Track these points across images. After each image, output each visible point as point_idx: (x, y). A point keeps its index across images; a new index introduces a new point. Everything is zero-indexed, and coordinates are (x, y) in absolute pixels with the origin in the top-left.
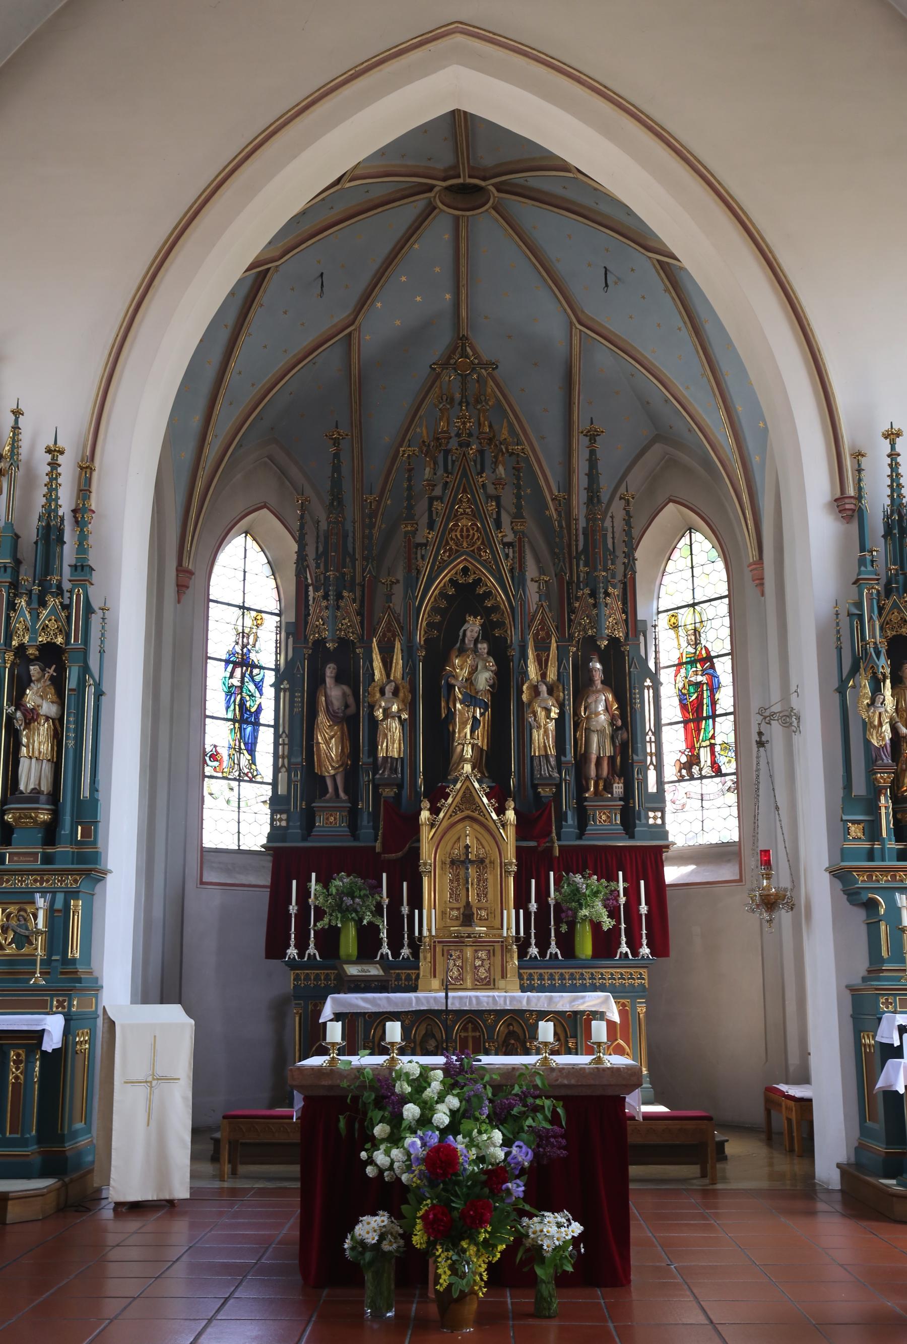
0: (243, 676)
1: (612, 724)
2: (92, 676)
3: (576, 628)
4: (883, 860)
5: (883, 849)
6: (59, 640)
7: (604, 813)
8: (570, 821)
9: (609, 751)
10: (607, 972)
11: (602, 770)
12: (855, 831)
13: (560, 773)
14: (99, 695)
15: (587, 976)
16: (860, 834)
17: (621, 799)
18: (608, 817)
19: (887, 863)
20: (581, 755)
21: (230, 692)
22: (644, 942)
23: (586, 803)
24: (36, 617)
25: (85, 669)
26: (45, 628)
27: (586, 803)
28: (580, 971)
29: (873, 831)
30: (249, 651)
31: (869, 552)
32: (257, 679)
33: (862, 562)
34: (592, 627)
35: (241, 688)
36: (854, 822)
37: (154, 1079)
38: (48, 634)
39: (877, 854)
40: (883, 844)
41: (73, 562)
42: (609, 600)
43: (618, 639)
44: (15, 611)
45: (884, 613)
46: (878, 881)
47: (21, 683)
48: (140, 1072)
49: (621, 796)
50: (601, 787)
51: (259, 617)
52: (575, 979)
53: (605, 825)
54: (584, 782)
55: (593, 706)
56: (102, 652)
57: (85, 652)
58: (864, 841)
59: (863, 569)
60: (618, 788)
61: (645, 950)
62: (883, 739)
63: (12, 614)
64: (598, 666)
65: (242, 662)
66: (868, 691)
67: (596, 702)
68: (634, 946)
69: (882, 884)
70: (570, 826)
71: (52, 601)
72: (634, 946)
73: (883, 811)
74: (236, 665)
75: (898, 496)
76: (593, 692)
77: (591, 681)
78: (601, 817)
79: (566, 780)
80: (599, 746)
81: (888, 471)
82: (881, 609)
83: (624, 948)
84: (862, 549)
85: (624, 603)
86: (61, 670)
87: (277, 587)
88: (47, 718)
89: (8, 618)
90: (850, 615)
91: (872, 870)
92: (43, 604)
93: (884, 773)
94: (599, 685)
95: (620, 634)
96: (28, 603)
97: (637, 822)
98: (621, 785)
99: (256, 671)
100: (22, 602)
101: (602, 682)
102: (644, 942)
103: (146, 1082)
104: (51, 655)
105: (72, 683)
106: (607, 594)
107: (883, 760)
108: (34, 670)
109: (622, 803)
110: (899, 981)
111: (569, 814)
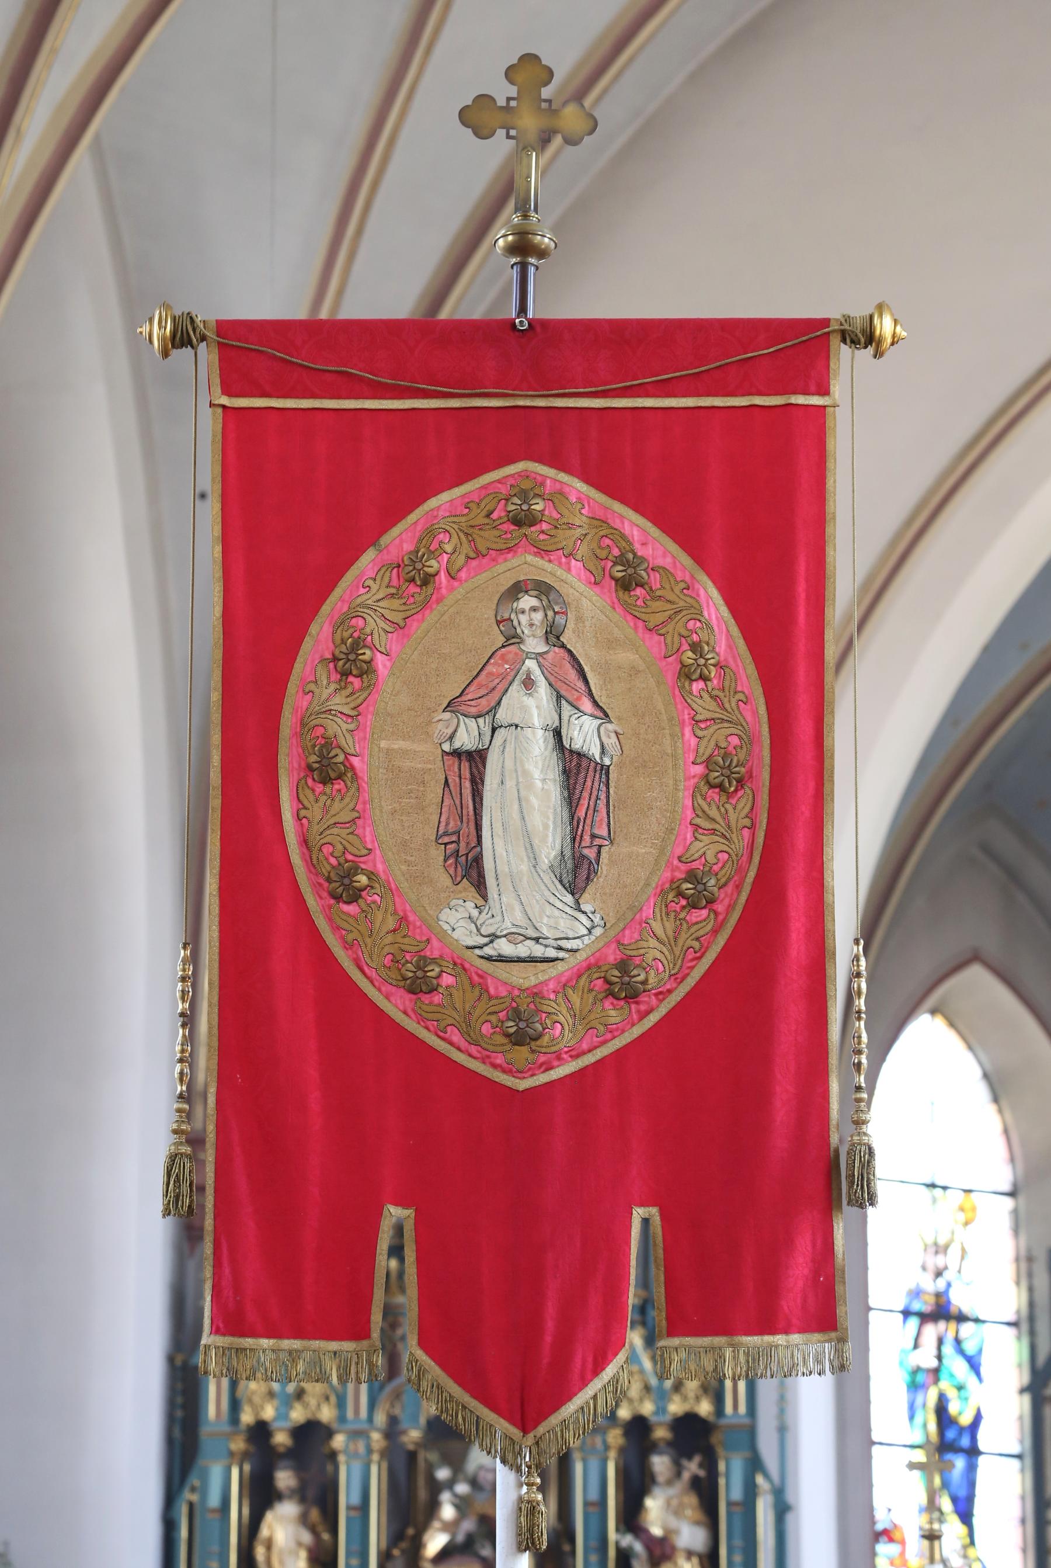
0: (940, 1342)
2: (767, 1476)
6: (705, 1408)
14: (782, 1510)
25: (755, 1464)
30: (949, 1285)
32: (970, 1348)
35: (936, 1372)
38: (685, 1399)
47: (635, 1488)
51: (967, 1206)
56: (782, 1430)
57: (751, 1432)
74: (925, 1318)
86: (710, 1464)
87: (1006, 1131)
88: (690, 1554)
99: (967, 1329)
104: (693, 1436)
105: (731, 1487)
108: (660, 1463)
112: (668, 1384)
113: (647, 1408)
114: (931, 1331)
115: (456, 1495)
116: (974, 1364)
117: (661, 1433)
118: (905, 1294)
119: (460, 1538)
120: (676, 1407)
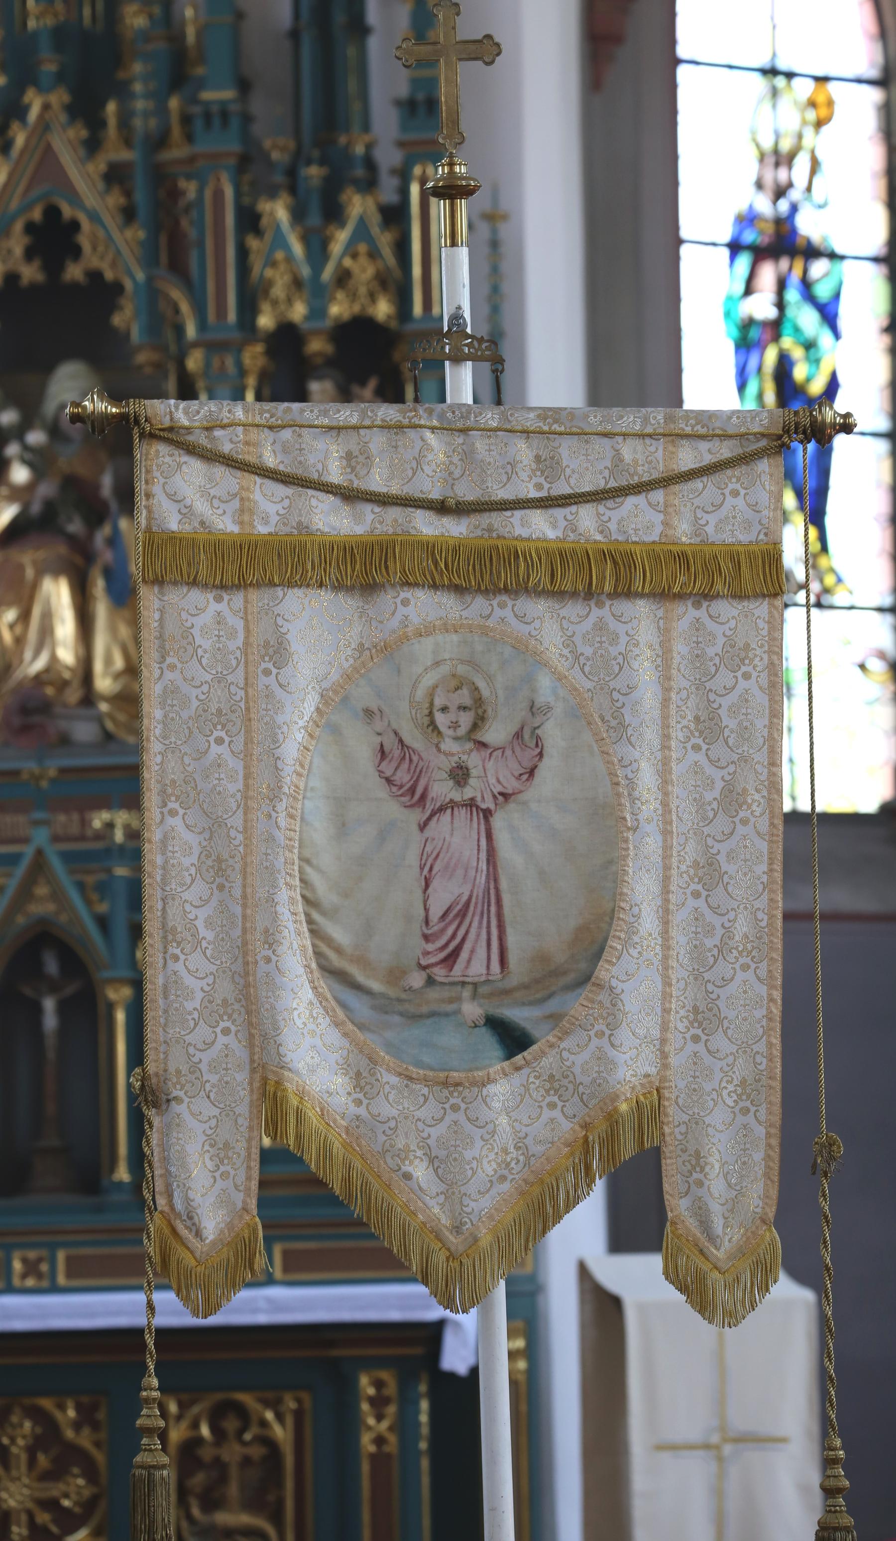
0: (782, 285)
6: (383, 309)
21: (750, 337)
24: (318, 249)
26: (343, 278)
30: (794, 208)
32: (823, 292)
35: (775, 328)
37: (725, 1440)
38: (353, 296)
41: (403, 90)
44: (258, 232)
48: (689, 1421)
51: (821, 99)
63: (253, 243)
65: (777, 244)
71: (358, 205)
74: (760, 254)
89: (243, 253)
92: (334, 213)
96: (298, 215)
99: (818, 268)
100: (278, 211)
103: (707, 1447)
112: (327, 274)
113: (298, 311)
114: (768, 274)
115: (26, 447)
116: (828, 315)
117: (316, 346)
118: (732, 219)
119: (36, 508)
120: (338, 309)
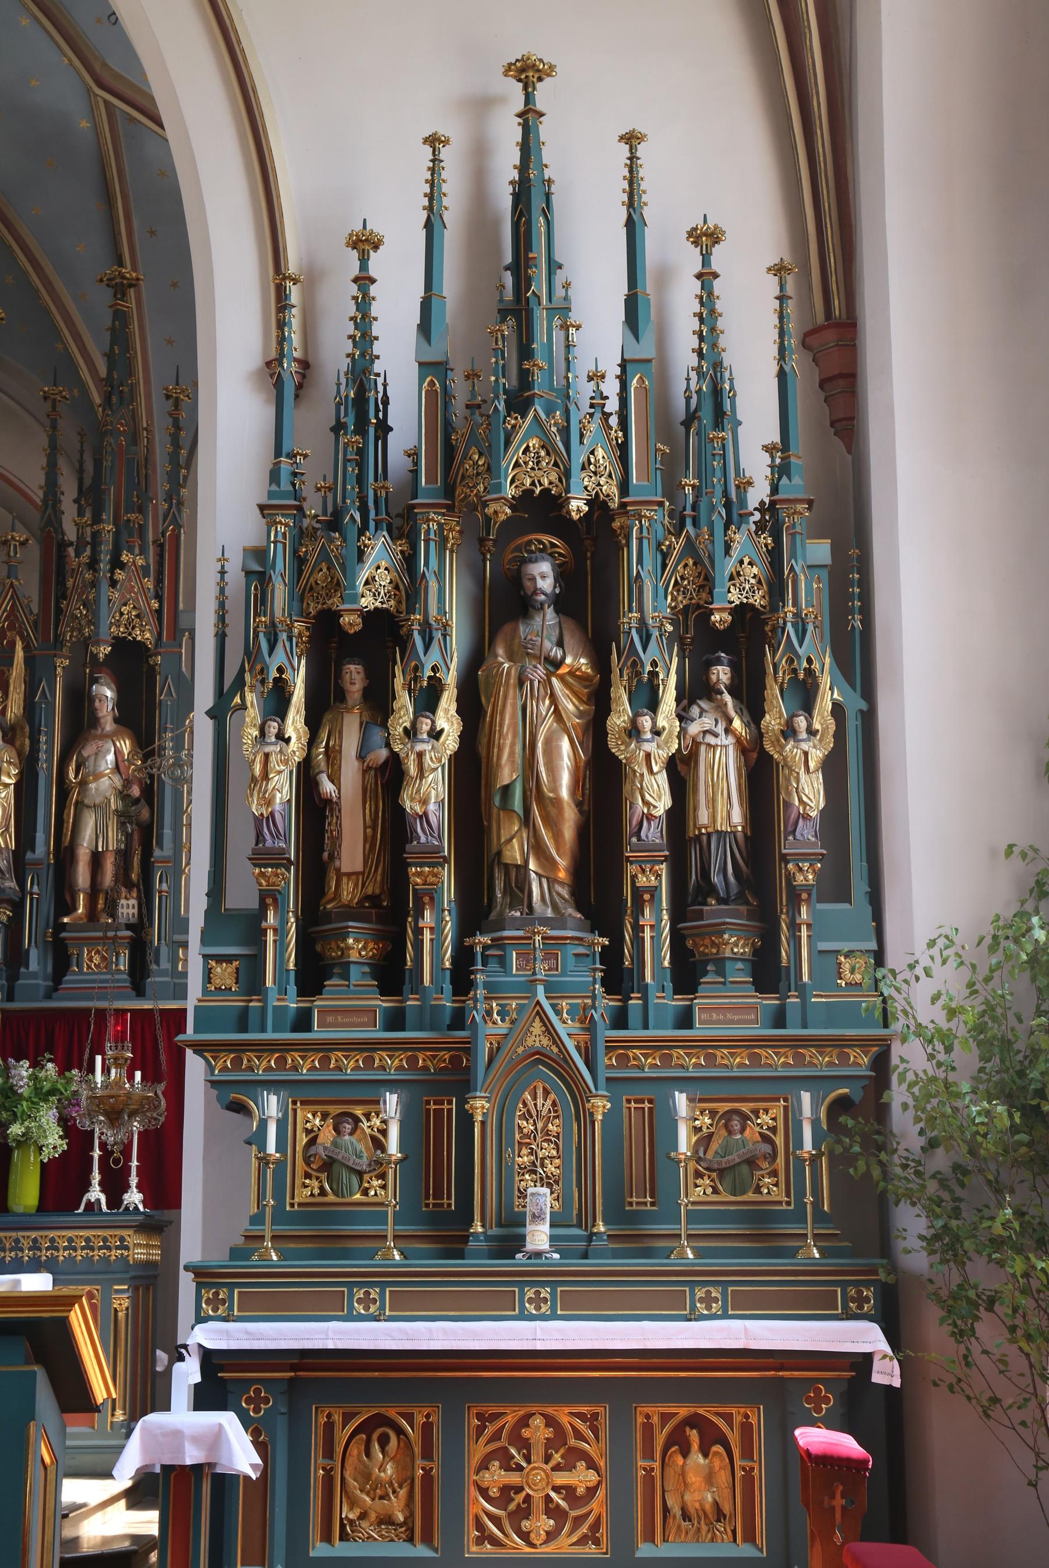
1: (123, 795)
3: (68, 625)
4: (263, 1030)
5: (263, 1010)
7: (98, 952)
8: (34, 965)
9: (113, 840)
10: (69, 1239)
11: (103, 875)
12: (224, 974)
13: (22, 883)
15: (25, 1244)
16: (230, 982)
17: (129, 927)
18: (104, 958)
19: (269, 1035)
20: (66, 848)
22: (134, 1180)
23: (63, 935)
27: (63, 935)
28: (13, 1234)
29: (251, 978)
31: (288, 456)
33: (274, 476)
34: (90, 623)
36: (220, 959)
39: (253, 1019)
40: (264, 1000)
42: (120, 575)
43: (140, 645)
45: (307, 570)
46: (339, 1068)
49: (132, 920)
50: (101, 905)
52: (22, 1250)
53: (98, 971)
54: (68, 898)
55: (90, 763)
58: (236, 993)
59: (274, 488)
60: (128, 908)
61: (134, 1197)
62: (269, 802)
64: (109, 693)
66: (253, 713)
67: (96, 754)
68: (115, 1187)
69: (260, 1074)
70: (34, 975)
72: (115, 1187)
73: (270, 937)
75: (363, 355)
76: (96, 737)
77: (95, 721)
78: (91, 959)
79: (32, 894)
80: (95, 834)
81: (352, 309)
82: (299, 561)
83: (96, 1194)
84: (278, 453)
85: (159, 581)
90: (248, 573)
91: (237, 1048)
93: (266, 866)
94: (109, 725)
95: (145, 635)
97: (154, 967)
98: (133, 902)
101: (116, 720)
102: (134, 1180)
106: (117, 564)
107: (265, 841)
109: (128, 933)
110: (794, 1257)
111: (34, 955)
